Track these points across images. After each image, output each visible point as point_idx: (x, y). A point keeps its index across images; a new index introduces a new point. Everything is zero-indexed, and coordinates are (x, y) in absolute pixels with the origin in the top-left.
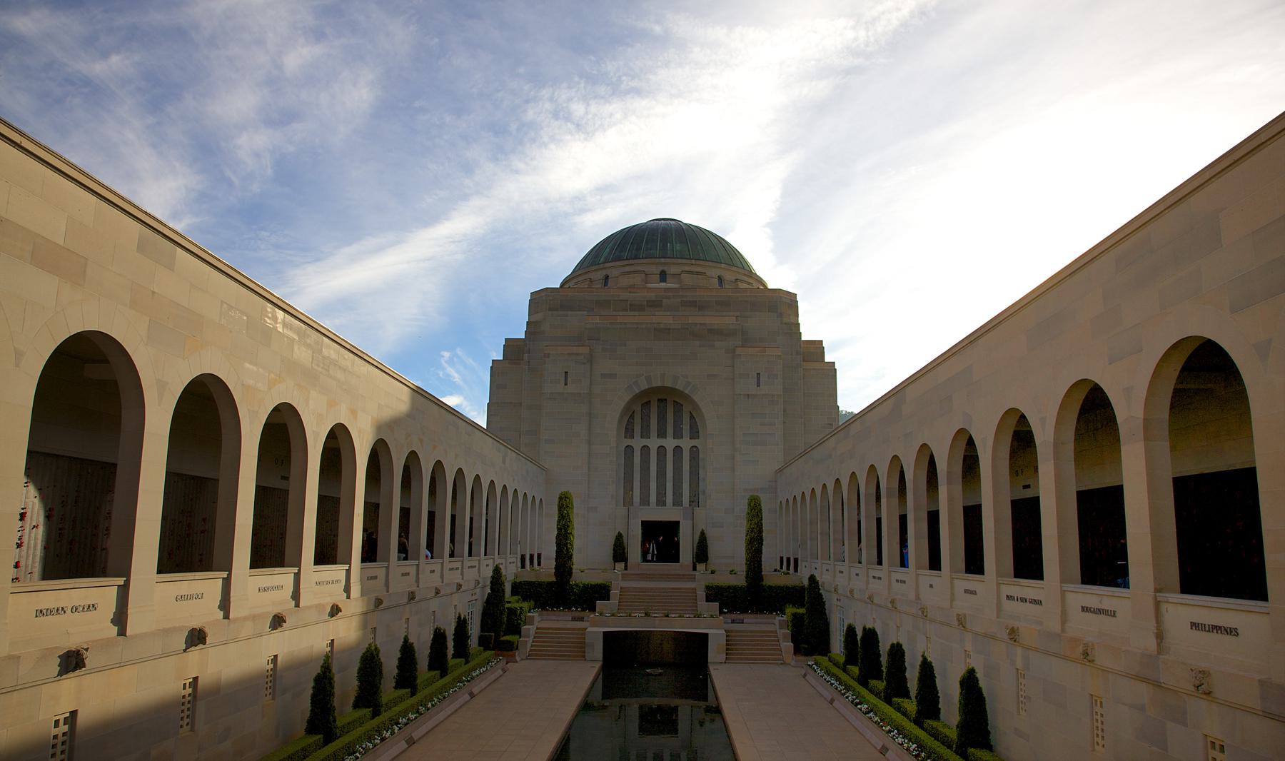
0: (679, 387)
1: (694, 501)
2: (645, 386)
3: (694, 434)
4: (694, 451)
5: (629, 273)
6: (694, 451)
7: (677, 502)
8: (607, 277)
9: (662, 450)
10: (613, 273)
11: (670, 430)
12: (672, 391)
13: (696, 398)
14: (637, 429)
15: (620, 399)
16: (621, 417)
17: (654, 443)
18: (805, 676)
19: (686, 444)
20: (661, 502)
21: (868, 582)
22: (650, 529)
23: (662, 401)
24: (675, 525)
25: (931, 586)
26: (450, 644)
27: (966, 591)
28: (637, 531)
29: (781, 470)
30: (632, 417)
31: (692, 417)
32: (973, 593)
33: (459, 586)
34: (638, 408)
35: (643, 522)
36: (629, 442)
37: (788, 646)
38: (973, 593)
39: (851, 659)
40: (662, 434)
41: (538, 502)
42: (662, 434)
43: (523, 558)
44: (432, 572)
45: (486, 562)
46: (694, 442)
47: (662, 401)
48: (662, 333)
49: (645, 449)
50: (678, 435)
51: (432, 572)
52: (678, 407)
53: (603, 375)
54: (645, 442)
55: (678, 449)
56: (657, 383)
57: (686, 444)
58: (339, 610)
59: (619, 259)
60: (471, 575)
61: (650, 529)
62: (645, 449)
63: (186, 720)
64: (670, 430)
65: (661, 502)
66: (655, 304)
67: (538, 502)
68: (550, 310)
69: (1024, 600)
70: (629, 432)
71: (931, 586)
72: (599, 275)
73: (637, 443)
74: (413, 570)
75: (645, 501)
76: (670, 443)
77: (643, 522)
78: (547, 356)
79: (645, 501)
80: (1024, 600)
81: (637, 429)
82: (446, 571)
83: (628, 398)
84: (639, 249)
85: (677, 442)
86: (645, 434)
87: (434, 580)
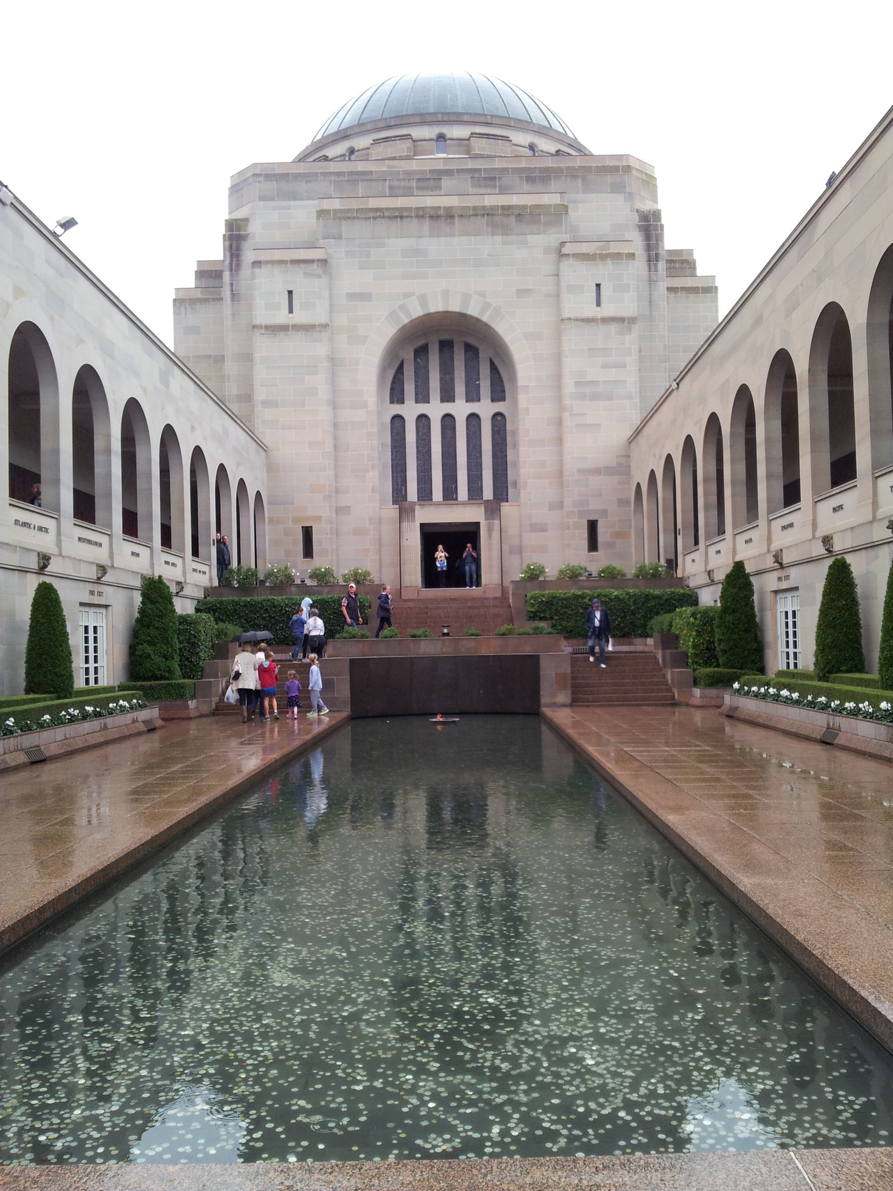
0: (472, 310)
1: (501, 492)
2: (417, 312)
3: (498, 394)
4: (499, 419)
5: (386, 139)
6: (499, 419)
7: (475, 491)
9: (448, 420)
11: (460, 389)
14: (409, 388)
16: (383, 370)
17: (435, 410)
19: (486, 409)
20: (450, 493)
22: (432, 536)
28: (414, 541)
29: (638, 432)
30: (400, 369)
31: (494, 368)
34: (409, 356)
36: (397, 409)
40: (448, 396)
42: (448, 396)
46: (499, 407)
47: (446, 346)
49: (423, 420)
50: (473, 395)
52: (471, 351)
53: (352, 296)
55: (473, 418)
56: (436, 306)
57: (486, 409)
61: (432, 536)
62: (423, 420)
64: (460, 389)
65: (450, 493)
68: (262, 198)
70: (397, 396)
73: (410, 410)
75: (425, 494)
76: (461, 409)
77: (422, 525)
79: (425, 494)
81: (409, 388)
85: (472, 408)
86: (422, 397)
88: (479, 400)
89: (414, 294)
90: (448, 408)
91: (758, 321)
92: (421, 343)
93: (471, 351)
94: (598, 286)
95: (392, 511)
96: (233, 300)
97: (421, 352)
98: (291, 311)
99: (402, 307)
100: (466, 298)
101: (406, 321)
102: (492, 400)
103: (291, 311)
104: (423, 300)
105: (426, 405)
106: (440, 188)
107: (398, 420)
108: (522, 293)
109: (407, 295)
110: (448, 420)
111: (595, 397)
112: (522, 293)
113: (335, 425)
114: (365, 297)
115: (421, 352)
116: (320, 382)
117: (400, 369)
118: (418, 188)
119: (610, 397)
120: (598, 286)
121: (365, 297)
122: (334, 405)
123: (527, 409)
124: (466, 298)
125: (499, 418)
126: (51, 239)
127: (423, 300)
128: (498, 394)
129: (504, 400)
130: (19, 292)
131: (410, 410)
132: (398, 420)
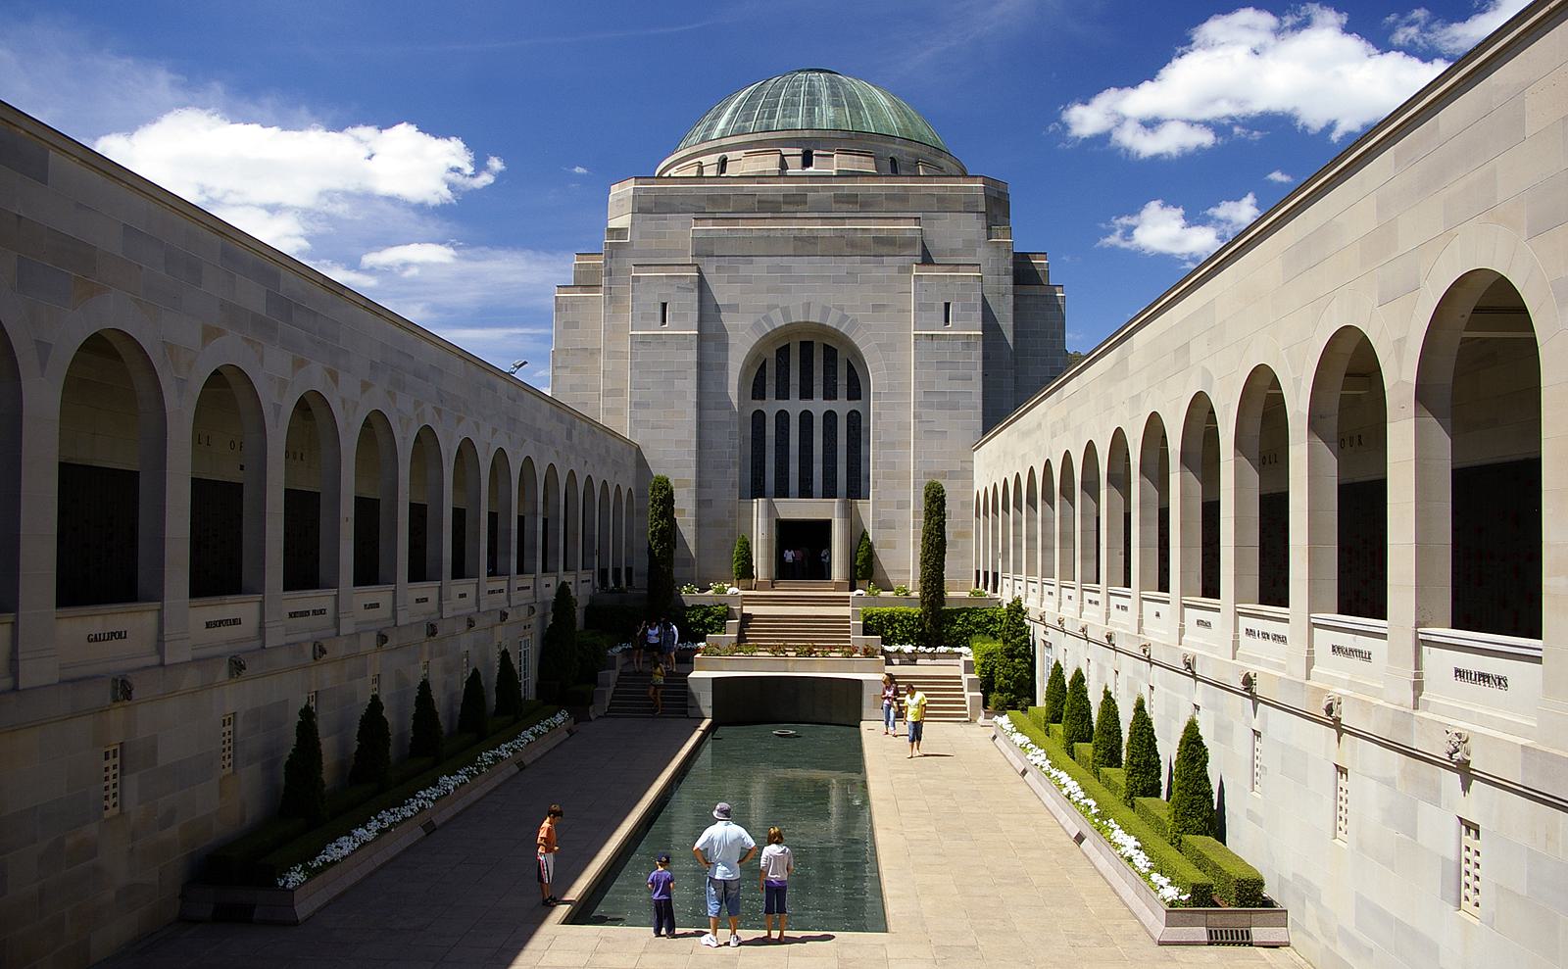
0: (831, 322)
1: (857, 489)
2: (779, 321)
3: (856, 390)
4: (856, 421)
8: (723, 163)
9: (806, 418)
10: (730, 155)
12: (822, 329)
17: (795, 406)
18: (994, 738)
19: (842, 406)
21: (1082, 609)
23: (807, 348)
24: (825, 526)
25: (1158, 615)
26: (492, 699)
27: (1200, 623)
30: (763, 367)
32: (1207, 625)
33: (504, 616)
36: (758, 405)
37: (971, 696)
38: (1207, 625)
39: (1055, 718)
41: (624, 494)
42: (806, 393)
43: (603, 573)
44: (463, 596)
45: (546, 581)
46: (854, 405)
47: (807, 348)
48: (805, 245)
49: (783, 417)
50: (830, 394)
51: (463, 596)
52: (830, 354)
54: (783, 405)
55: (830, 417)
56: (798, 317)
57: (842, 406)
58: (323, 651)
59: (742, 132)
60: (519, 598)
62: (783, 417)
63: (112, 801)
66: (796, 200)
67: (624, 494)
69: (1266, 636)
70: (758, 392)
71: (1158, 615)
72: (715, 158)
73: (771, 406)
74: (433, 596)
76: (818, 406)
78: (636, 279)
80: (1266, 636)
82: (483, 593)
83: (754, 339)
84: (772, 116)
85: (829, 405)
86: (783, 393)
87: (467, 606)
89: (777, 306)
91: (1039, 425)
94: (947, 305)
96: (610, 303)
97: (783, 353)
99: (767, 319)
100: (826, 311)
103: (664, 321)
104: (785, 312)
105: (786, 401)
106: (806, 203)
107: (759, 418)
108: (876, 307)
109: (771, 307)
110: (806, 418)
111: (941, 406)
112: (876, 307)
113: (700, 425)
114: (733, 308)
116: (690, 386)
117: (763, 367)
118: (785, 203)
119: (954, 407)
120: (947, 305)
121: (733, 308)
122: (700, 406)
123: (878, 415)
124: (826, 311)
125: (855, 415)
126: (508, 377)
127: (785, 312)
130: (495, 431)
131: (771, 406)
132: (759, 418)
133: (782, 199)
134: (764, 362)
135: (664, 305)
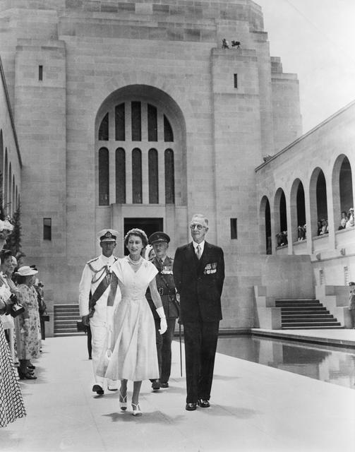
0: (158, 85)
3: (169, 136)
6: (169, 152)
13: (175, 95)
14: (112, 130)
15: (99, 95)
17: (129, 145)
30: (106, 120)
35: (125, 219)
36: (103, 144)
47: (136, 107)
52: (153, 112)
55: (153, 152)
57: (161, 146)
70: (103, 134)
73: (112, 145)
76: (145, 146)
77: (125, 219)
81: (112, 130)
83: (106, 94)
85: (152, 145)
88: (156, 140)
90: (137, 144)
92: (122, 102)
93: (153, 112)
95: (103, 210)
98: (41, 78)
101: (116, 89)
102: (166, 140)
103: (41, 78)
106: (134, 9)
115: (121, 108)
117: (106, 120)
128: (169, 136)
129: (172, 140)
131: (112, 145)
132: (104, 153)
133: (117, 6)
134: (108, 114)
135: (41, 67)
